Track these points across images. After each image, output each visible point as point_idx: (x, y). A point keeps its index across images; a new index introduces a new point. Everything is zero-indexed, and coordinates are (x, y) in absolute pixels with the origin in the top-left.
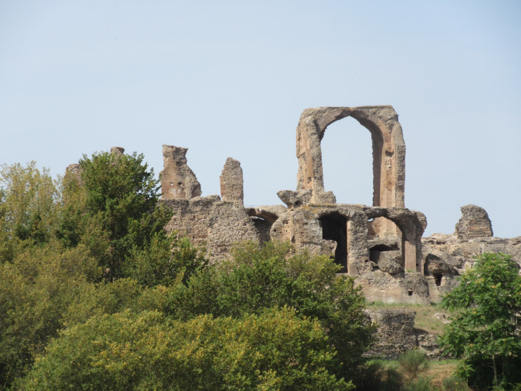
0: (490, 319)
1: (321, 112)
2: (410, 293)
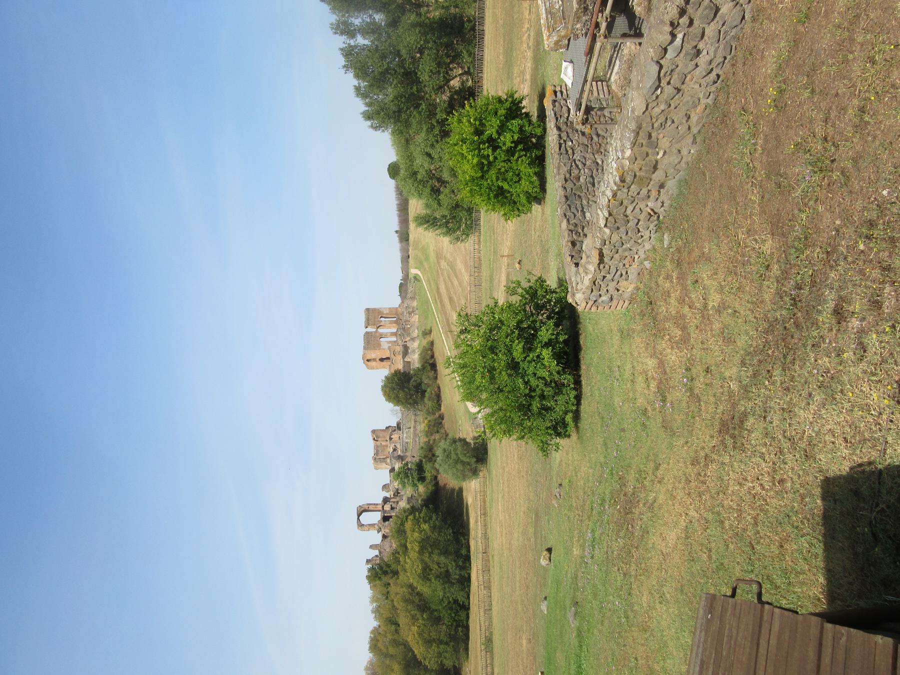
0: (409, 477)
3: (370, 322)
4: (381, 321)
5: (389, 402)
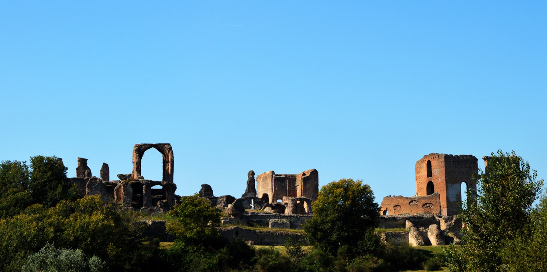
1: (141, 146)
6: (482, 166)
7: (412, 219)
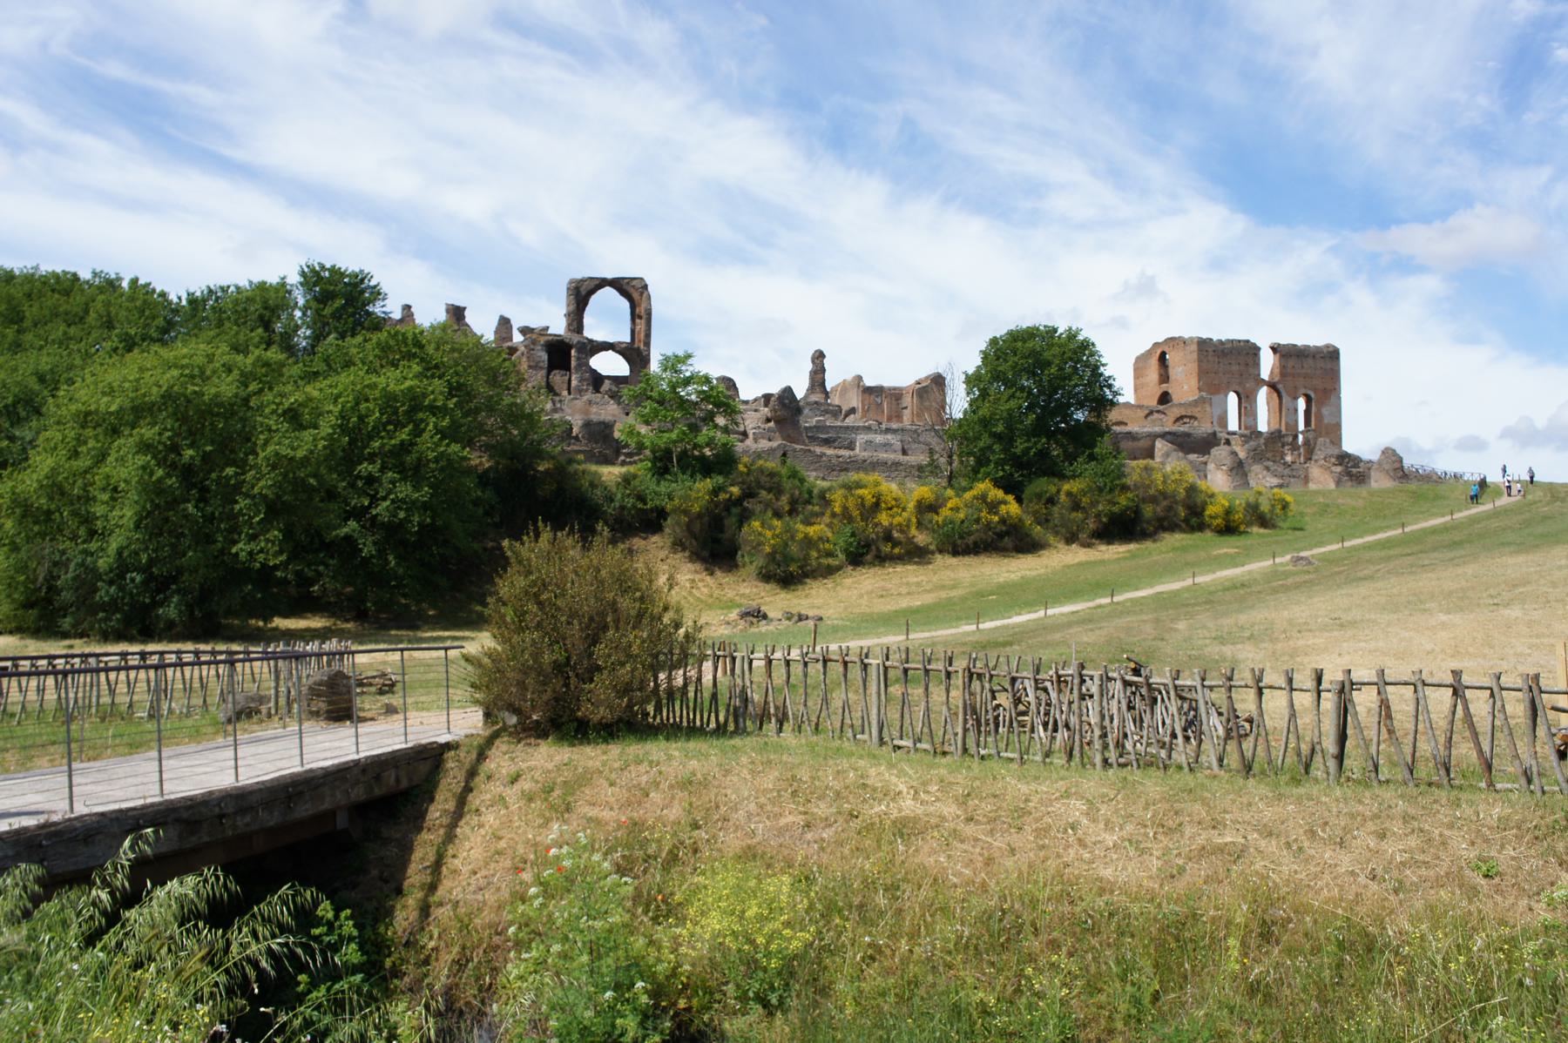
2: (627, 414)
3: (1291, 363)
4: (1296, 398)
5: (985, 356)
6: (1267, 364)
7: (1169, 437)
